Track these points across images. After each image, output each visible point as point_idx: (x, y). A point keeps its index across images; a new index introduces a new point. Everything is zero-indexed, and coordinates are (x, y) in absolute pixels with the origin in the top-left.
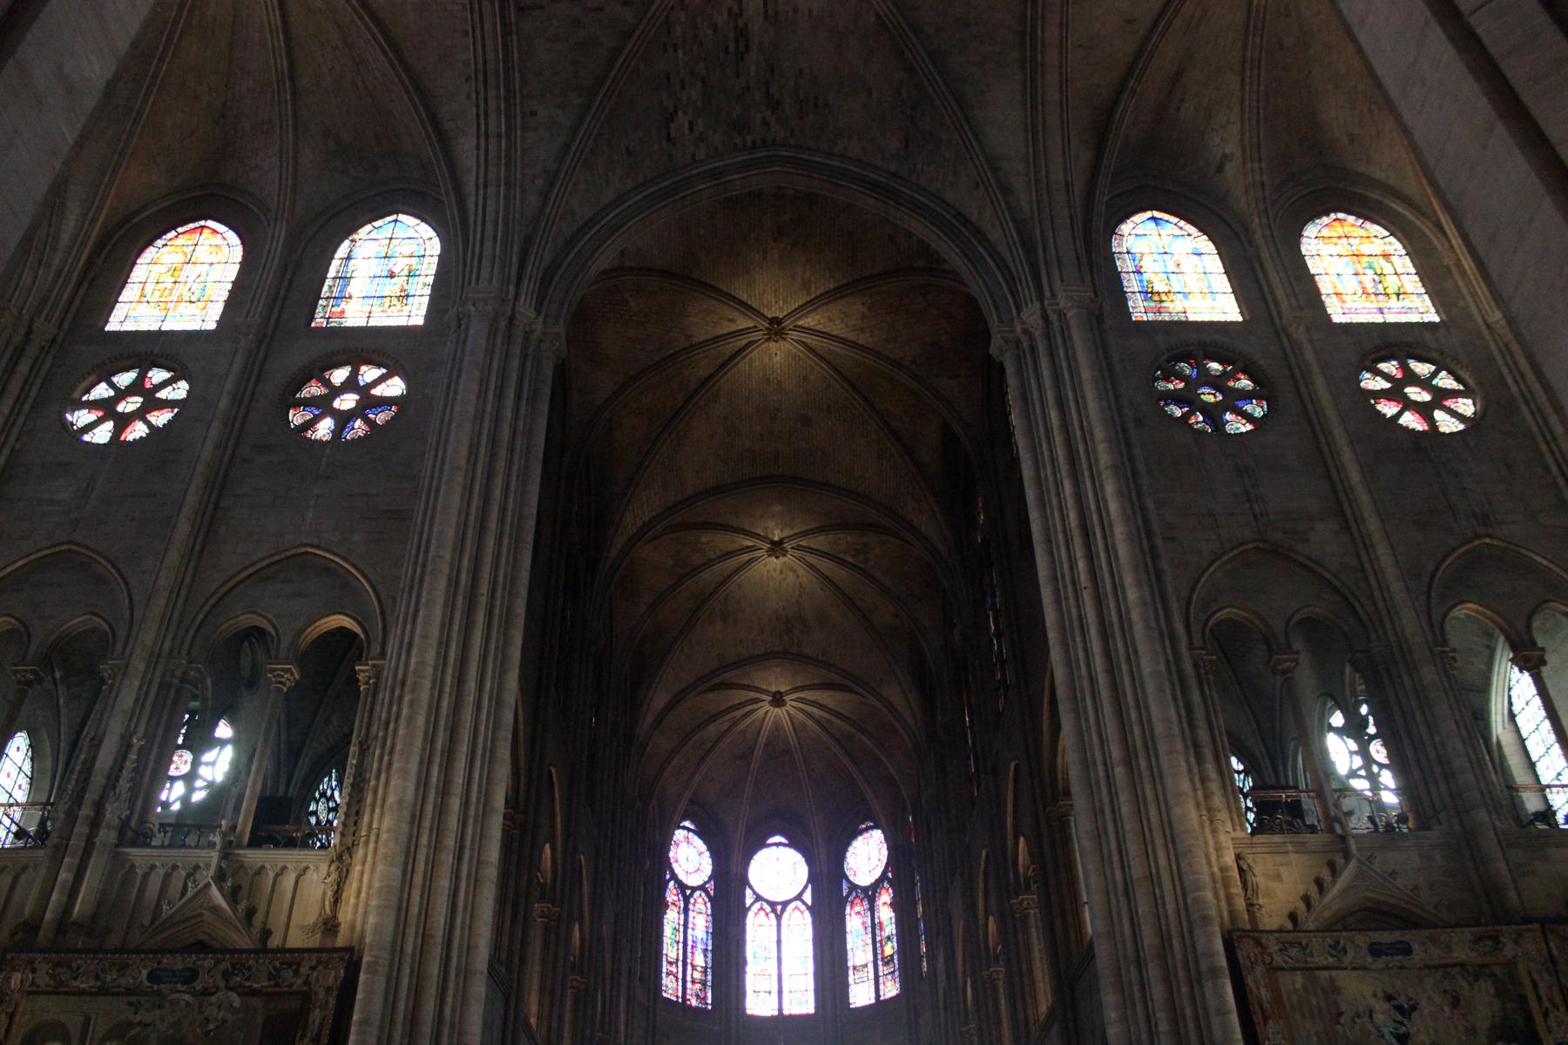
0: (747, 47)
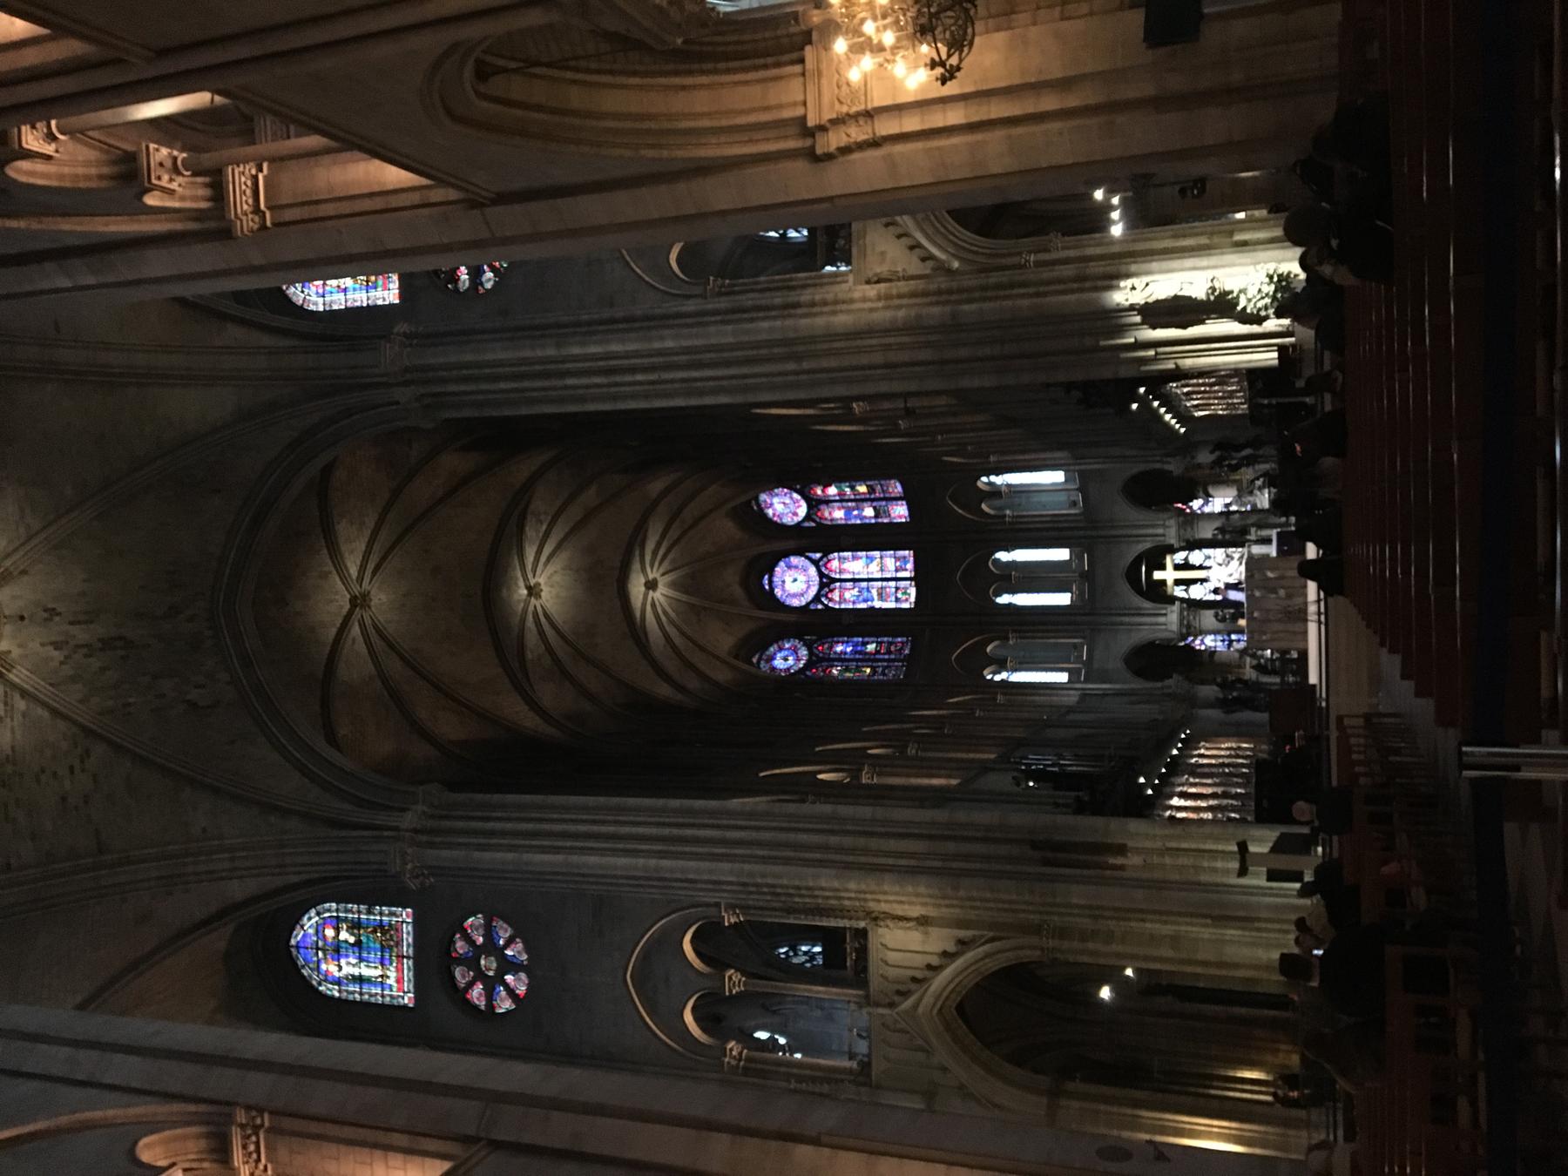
0: (120, 638)
